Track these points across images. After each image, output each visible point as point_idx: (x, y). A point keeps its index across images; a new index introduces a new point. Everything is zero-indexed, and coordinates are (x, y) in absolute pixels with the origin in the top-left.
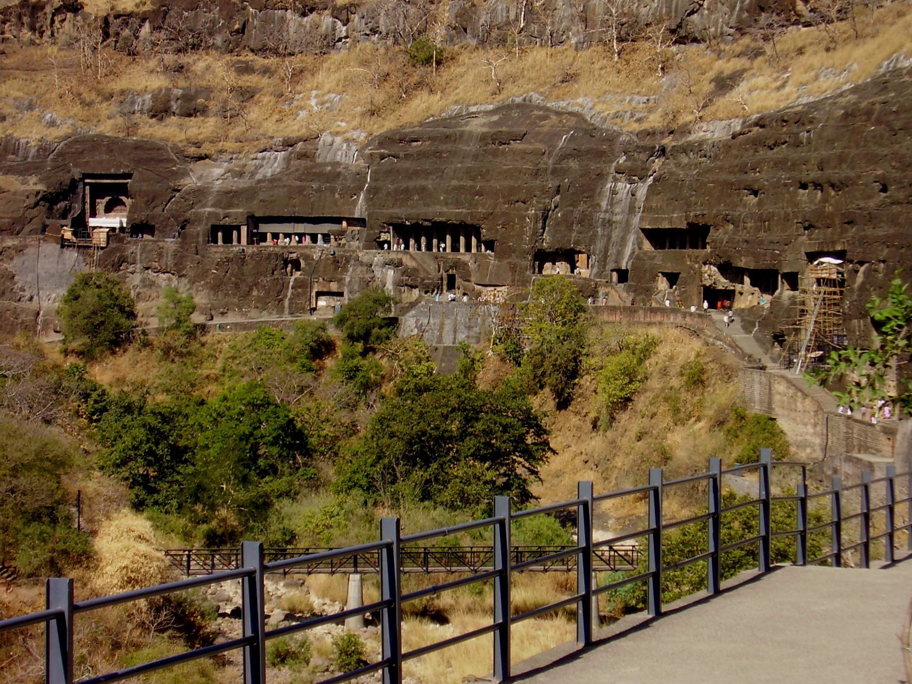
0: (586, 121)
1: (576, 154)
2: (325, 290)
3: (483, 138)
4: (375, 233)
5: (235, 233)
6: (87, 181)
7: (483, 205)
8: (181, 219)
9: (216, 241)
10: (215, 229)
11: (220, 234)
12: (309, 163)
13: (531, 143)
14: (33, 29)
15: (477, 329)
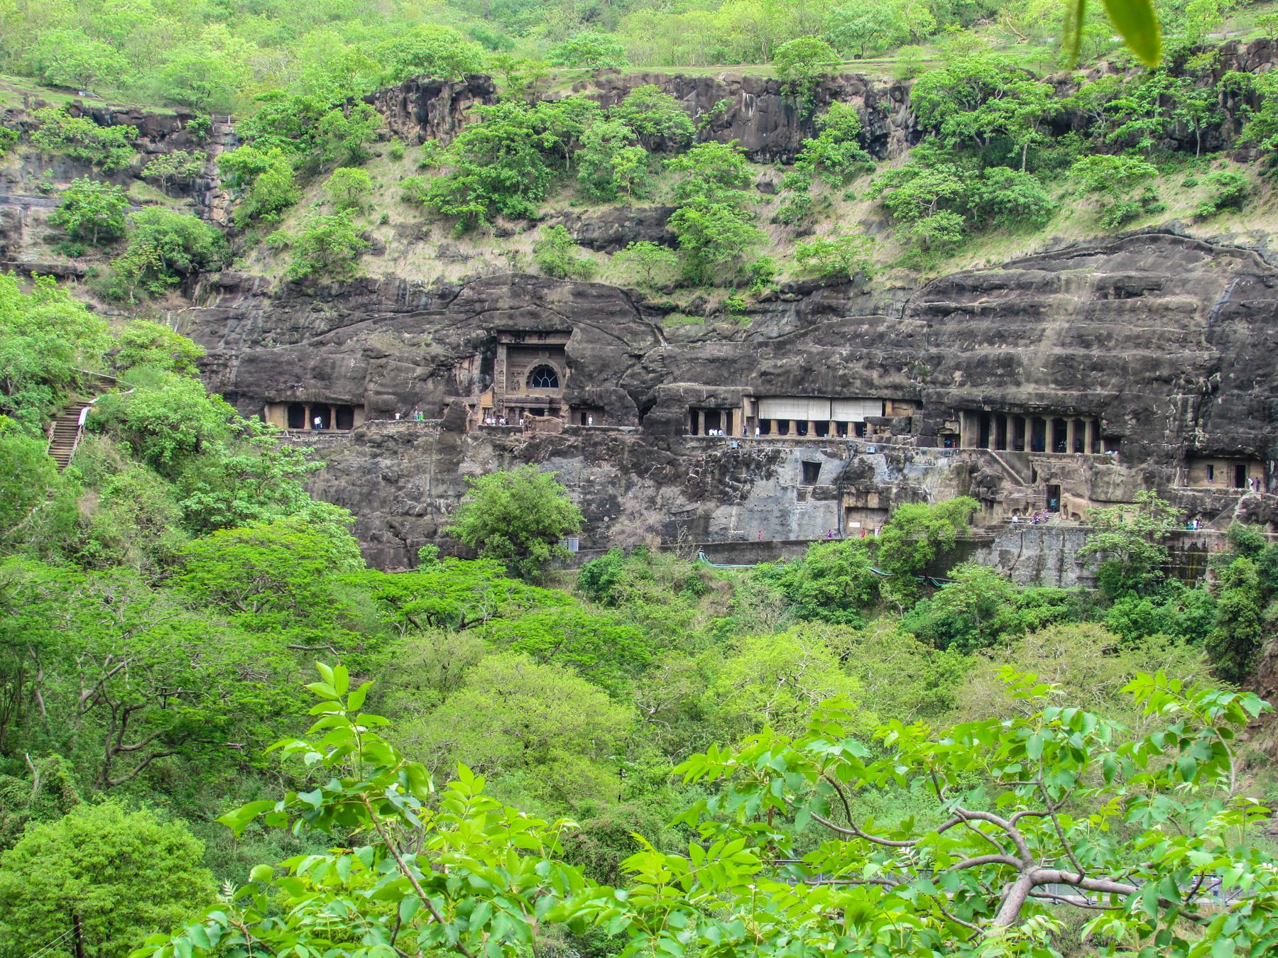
0: (1257, 264)
1: (1247, 313)
2: (860, 505)
3: (1101, 288)
4: (936, 423)
5: (724, 419)
6: (505, 340)
7: (1103, 385)
8: (644, 398)
9: (695, 432)
10: (694, 412)
11: (702, 419)
12: (835, 320)
13: (1174, 294)
14: (423, 120)
15: (1094, 568)
